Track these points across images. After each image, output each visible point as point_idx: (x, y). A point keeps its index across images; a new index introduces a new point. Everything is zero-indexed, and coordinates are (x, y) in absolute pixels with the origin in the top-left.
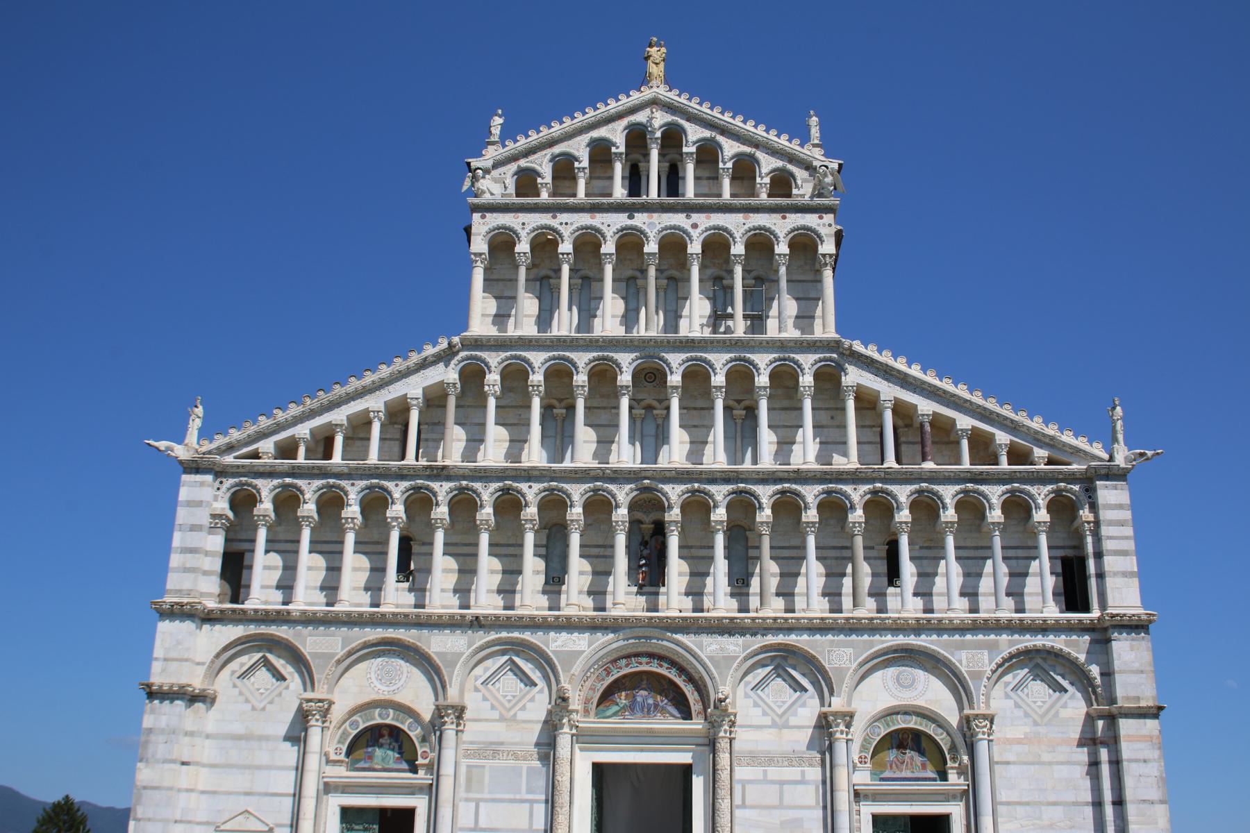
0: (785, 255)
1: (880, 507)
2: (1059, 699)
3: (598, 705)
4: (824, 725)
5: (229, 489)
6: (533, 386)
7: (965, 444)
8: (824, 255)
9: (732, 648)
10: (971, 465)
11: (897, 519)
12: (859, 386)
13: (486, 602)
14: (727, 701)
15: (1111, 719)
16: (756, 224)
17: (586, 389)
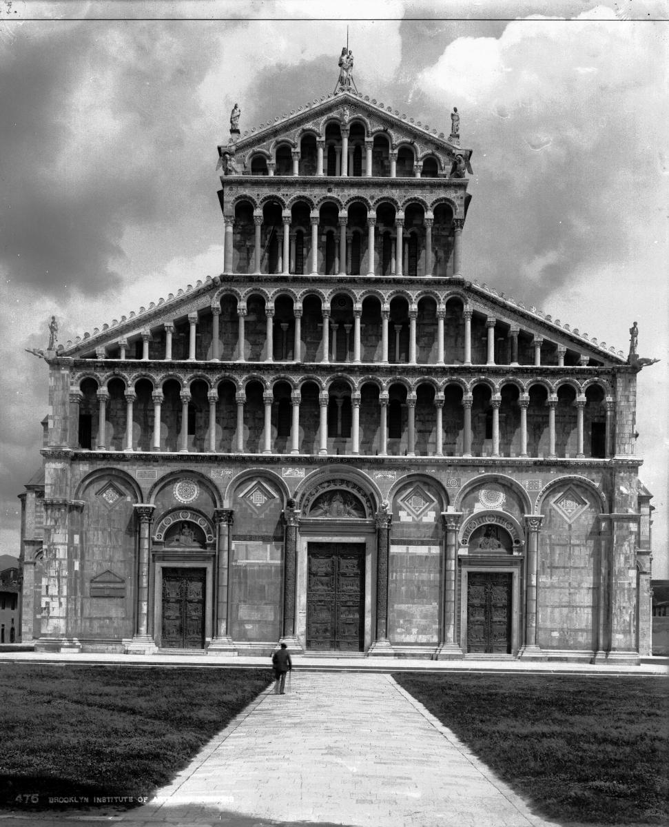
0: (431, 219)
1: (482, 391)
2: (582, 508)
3: (311, 510)
4: (443, 520)
5: (79, 378)
6: (268, 310)
7: (538, 351)
8: (457, 220)
9: (390, 476)
10: (541, 364)
11: (493, 399)
12: (475, 312)
13: (240, 449)
14: (387, 508)
15: (610, 521)
16: (412, 197)
17: (302, 312)
